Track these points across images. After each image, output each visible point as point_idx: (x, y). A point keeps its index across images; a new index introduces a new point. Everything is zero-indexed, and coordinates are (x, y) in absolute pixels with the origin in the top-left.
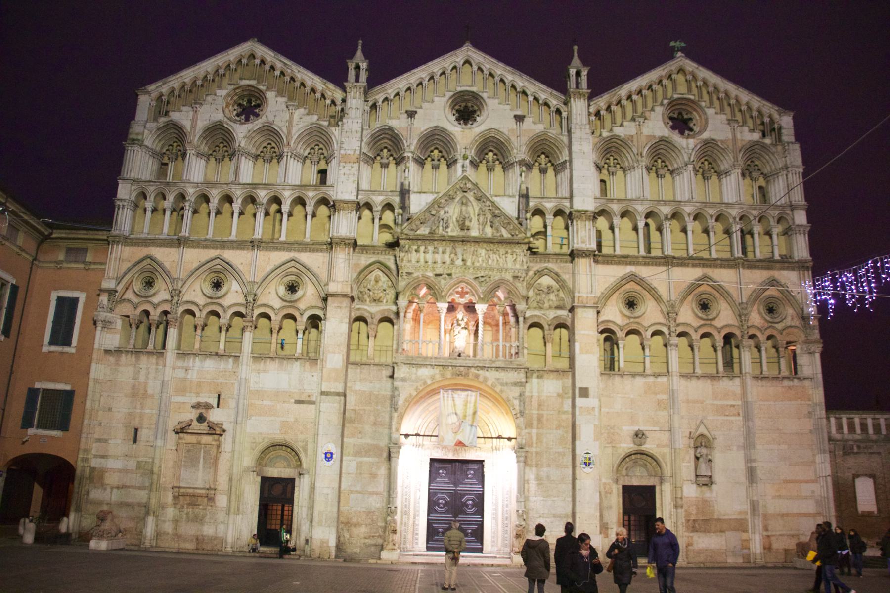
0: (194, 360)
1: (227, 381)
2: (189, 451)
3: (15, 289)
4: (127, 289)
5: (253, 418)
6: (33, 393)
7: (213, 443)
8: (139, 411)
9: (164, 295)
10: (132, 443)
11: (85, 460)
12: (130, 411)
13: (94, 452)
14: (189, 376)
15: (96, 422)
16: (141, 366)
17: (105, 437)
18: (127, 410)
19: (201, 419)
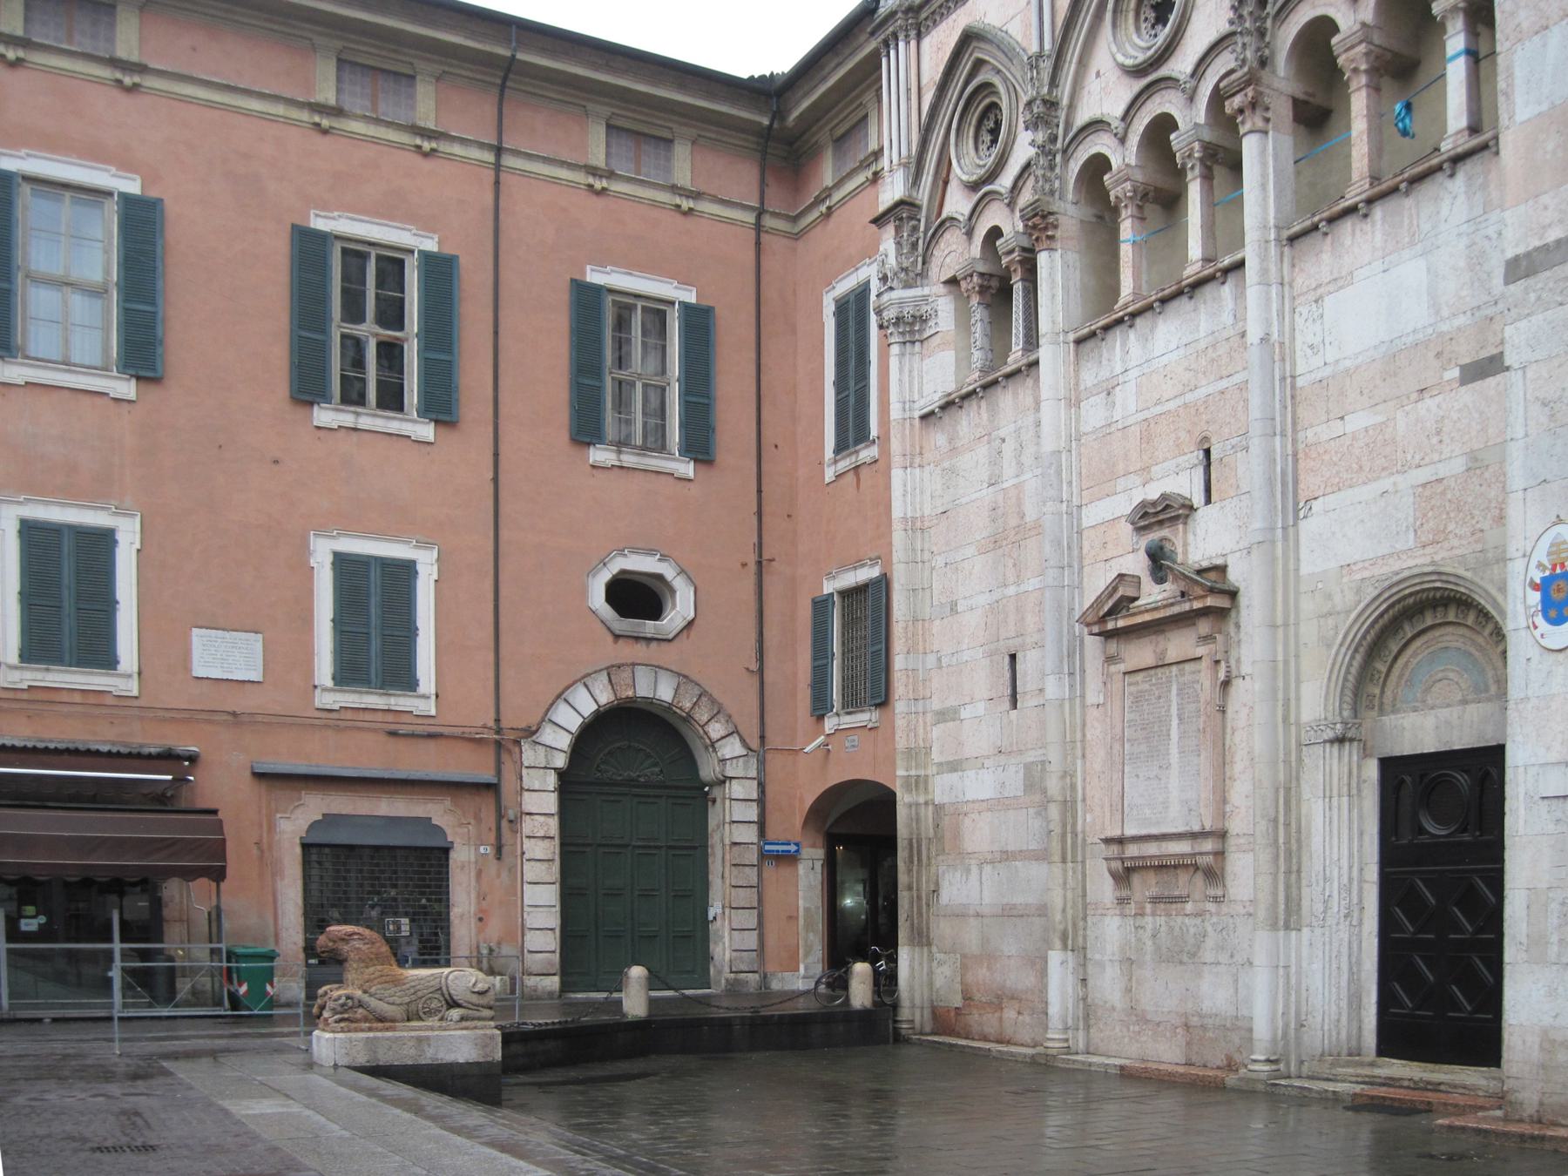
0: (1124, 344)
1: (1224, 384)
2: (1138, 699)
3: (698, 321)
4: (946, 183)
5: (1316, 505)
6: (821, 606)
7: (1201, 651)
8: (1011, 590)
9: (1024, 148)
10: (1007, 705)
11: (919, 783)
12: (996, 595)
13: (936, 756)
14: (1117, 415)
15: (931, 660)
16: (1002, 433)
17: (951, 702)
18: (983, 600)
19: (1159, 560)
